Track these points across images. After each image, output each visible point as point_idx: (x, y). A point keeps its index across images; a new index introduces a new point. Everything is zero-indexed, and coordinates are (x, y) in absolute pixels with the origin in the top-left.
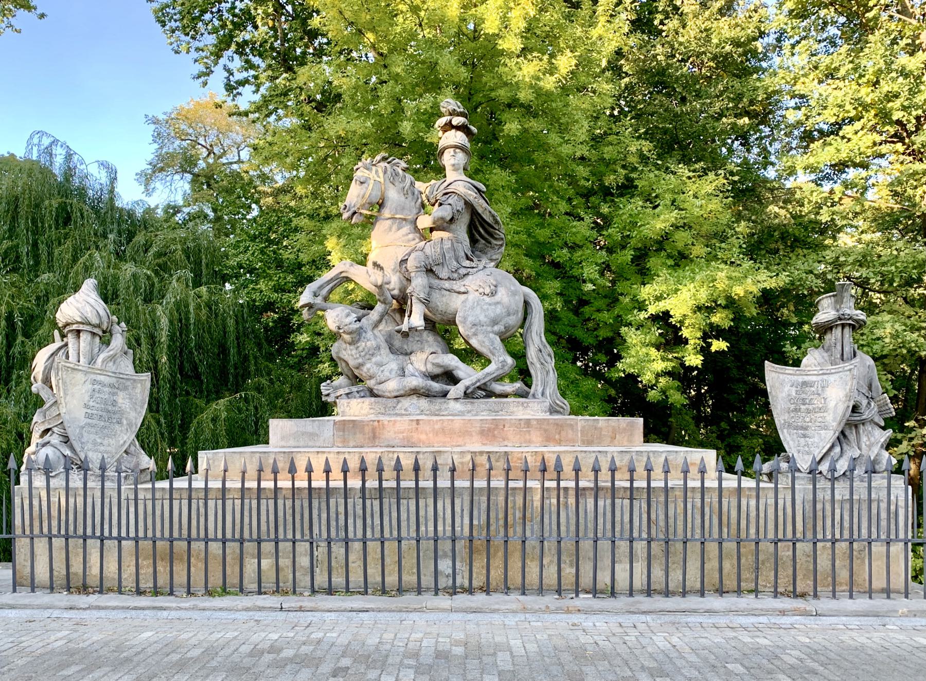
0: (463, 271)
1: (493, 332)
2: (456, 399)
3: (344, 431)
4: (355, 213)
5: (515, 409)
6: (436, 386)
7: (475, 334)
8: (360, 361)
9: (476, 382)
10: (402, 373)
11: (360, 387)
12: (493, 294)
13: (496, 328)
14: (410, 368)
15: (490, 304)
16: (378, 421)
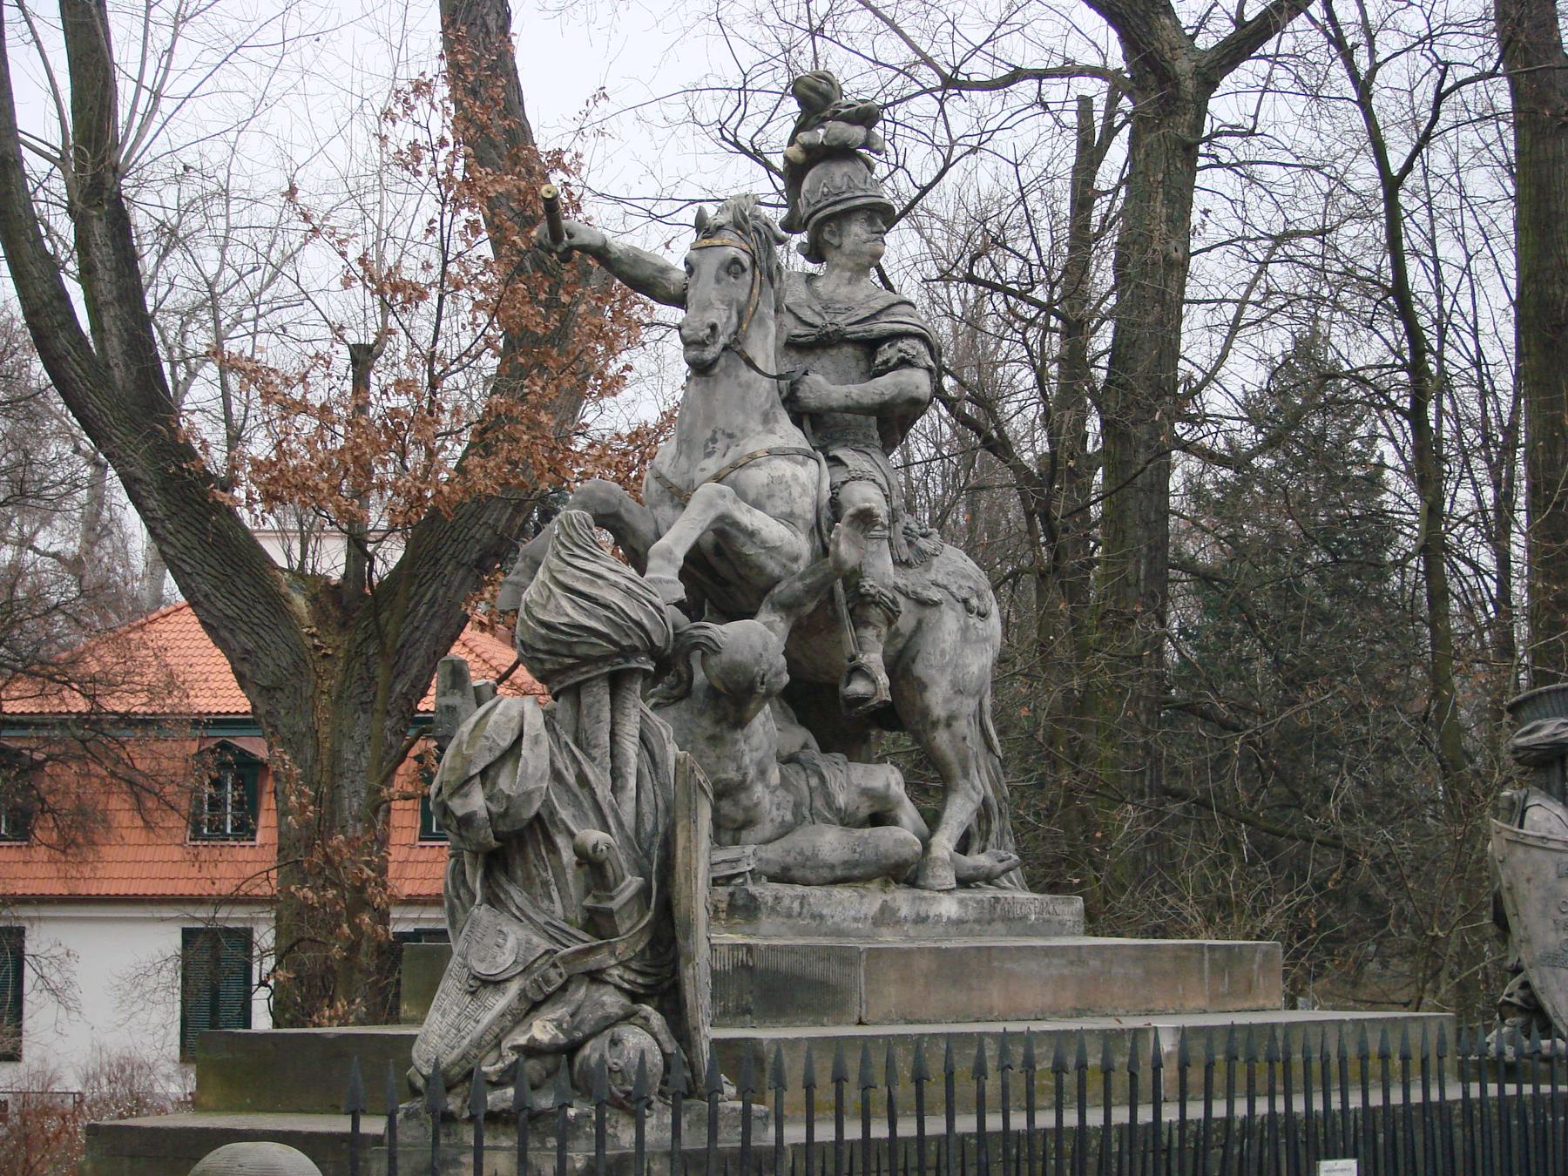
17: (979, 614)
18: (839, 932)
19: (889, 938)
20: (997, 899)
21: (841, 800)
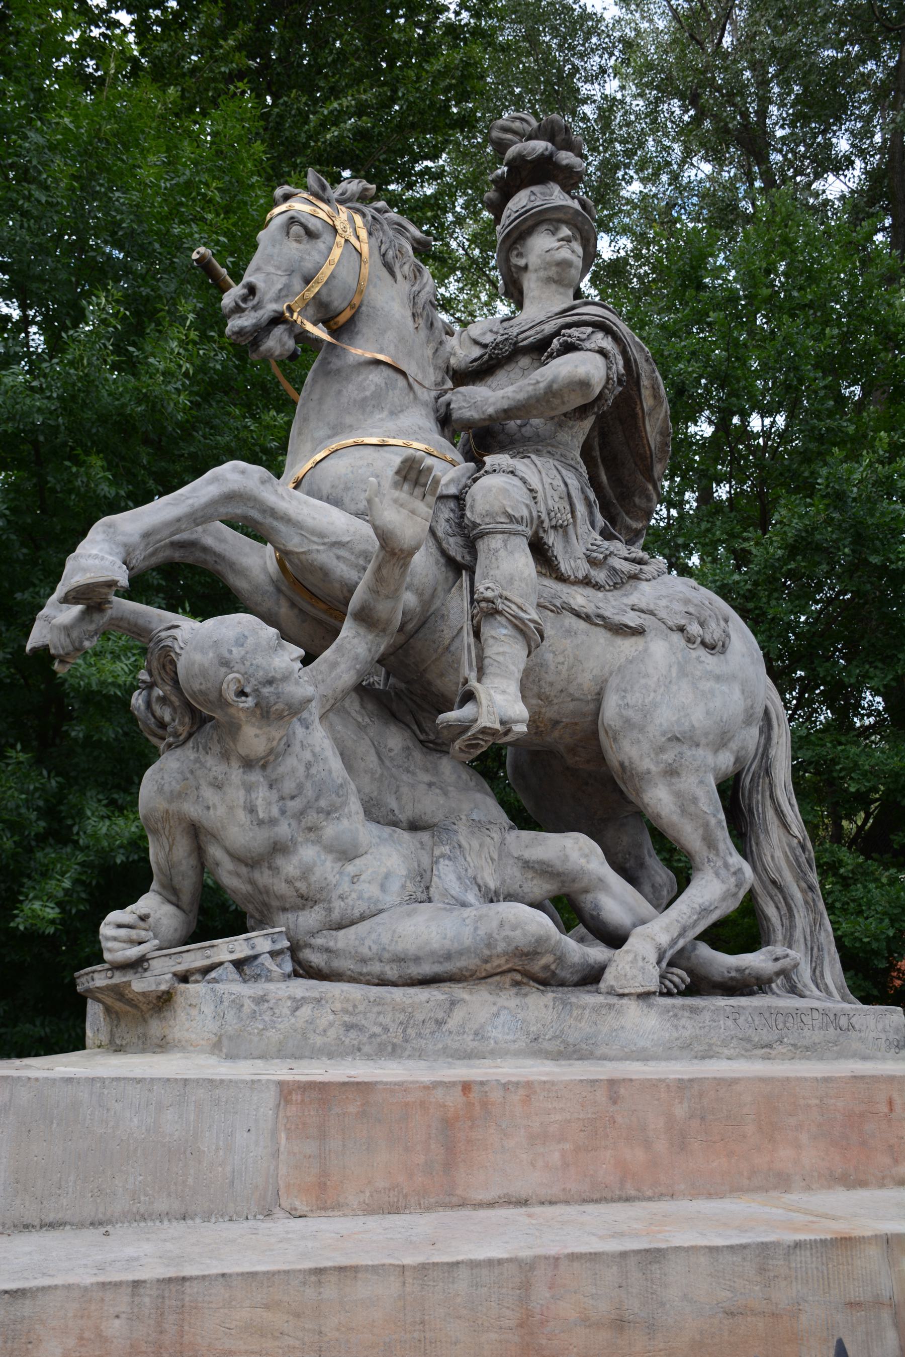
2: (644, 996)
3: (323, 1136)
4: (277, 320)
5: (817, 1036)
7: (671, 772)
8: (284, 830)
10: (422, 891)
11: (258, 942)
14: (447, 877)
15: (718, 678)
16: (466, 1087)
17: (703, 643)
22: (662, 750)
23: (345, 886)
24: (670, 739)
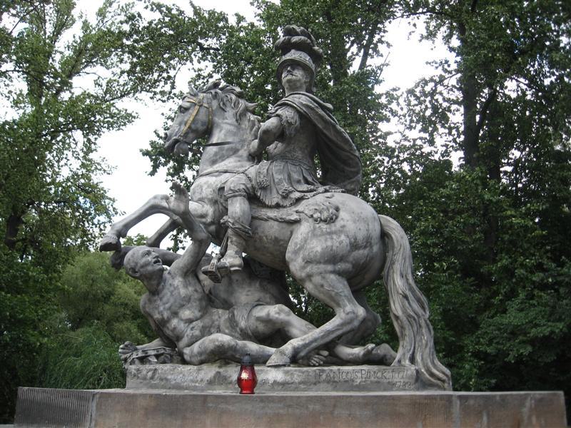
0: (297, 195)
1: (333, 272)
6: (253, 347)
9: (311, 342)
12: (331, 220)
13: (342, 266)
18: (178, 387)
19: (219, 391)
20: (323, 371)
21: (243, 324)
22: (304, 268)
23: (188, 331)
24: (306, 263)
